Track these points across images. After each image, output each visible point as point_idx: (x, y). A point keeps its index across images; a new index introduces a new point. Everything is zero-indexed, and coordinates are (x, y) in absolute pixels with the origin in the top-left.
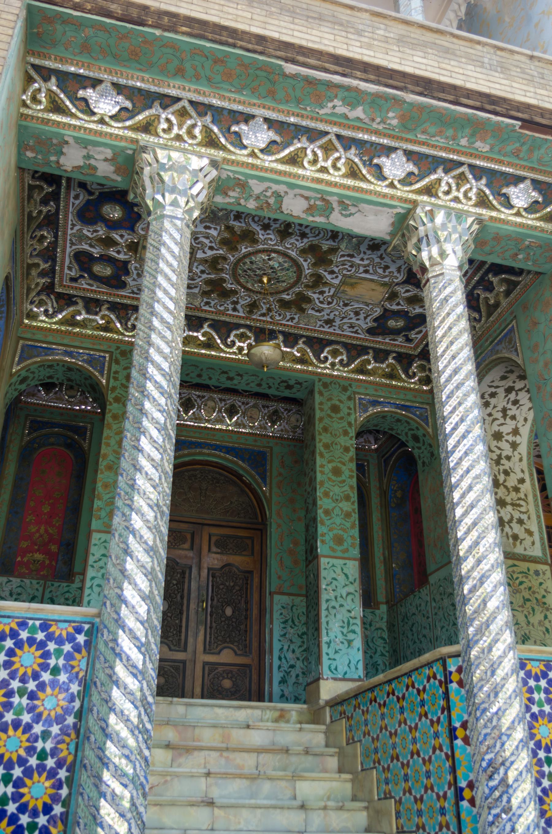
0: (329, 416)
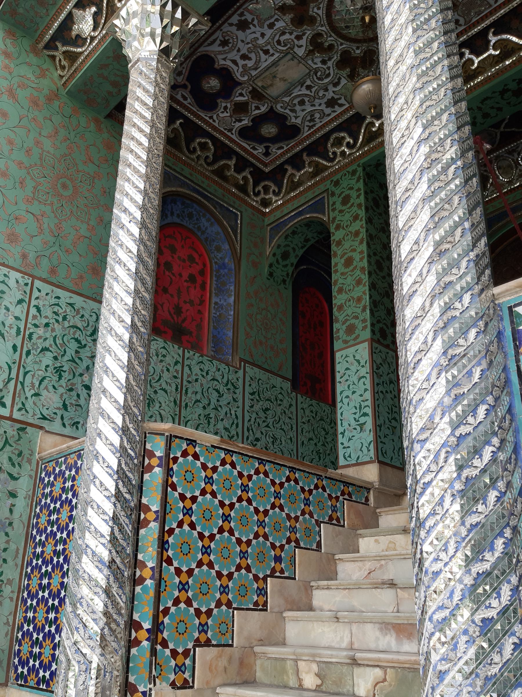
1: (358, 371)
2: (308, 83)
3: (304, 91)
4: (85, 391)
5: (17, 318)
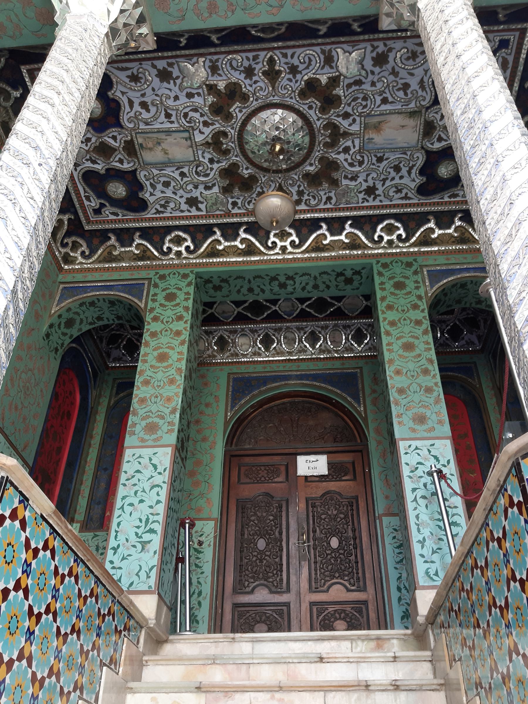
0: (392, 294)
1: (152, 477)
2: (185, 170)
3: (176, 175)
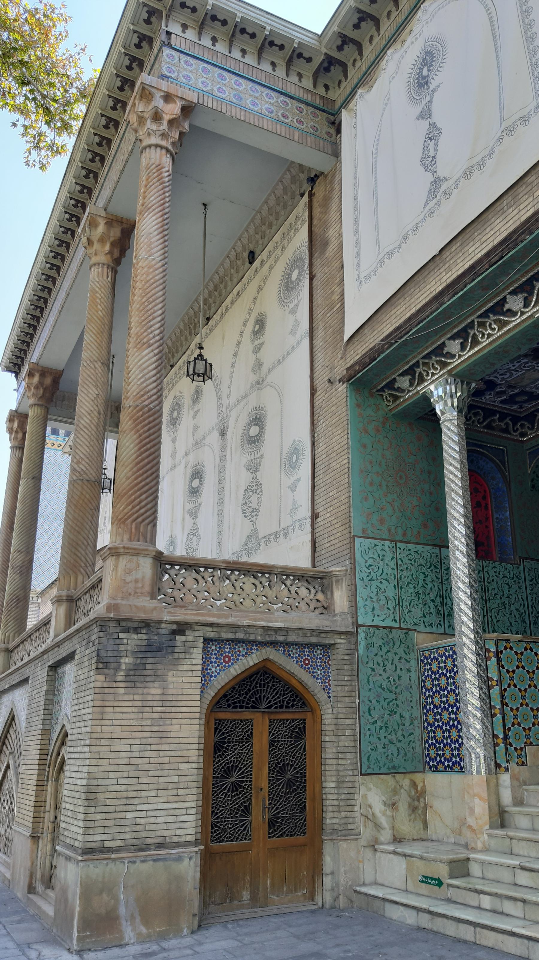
4: (432, 603)
5: (393, 569)
